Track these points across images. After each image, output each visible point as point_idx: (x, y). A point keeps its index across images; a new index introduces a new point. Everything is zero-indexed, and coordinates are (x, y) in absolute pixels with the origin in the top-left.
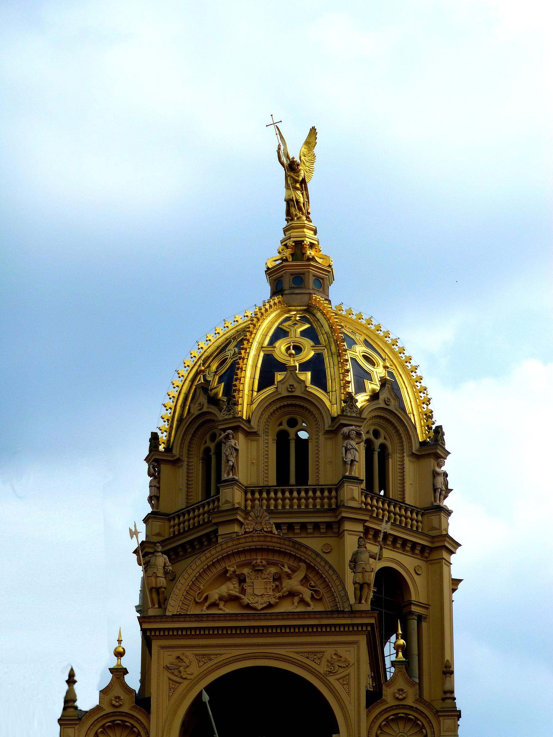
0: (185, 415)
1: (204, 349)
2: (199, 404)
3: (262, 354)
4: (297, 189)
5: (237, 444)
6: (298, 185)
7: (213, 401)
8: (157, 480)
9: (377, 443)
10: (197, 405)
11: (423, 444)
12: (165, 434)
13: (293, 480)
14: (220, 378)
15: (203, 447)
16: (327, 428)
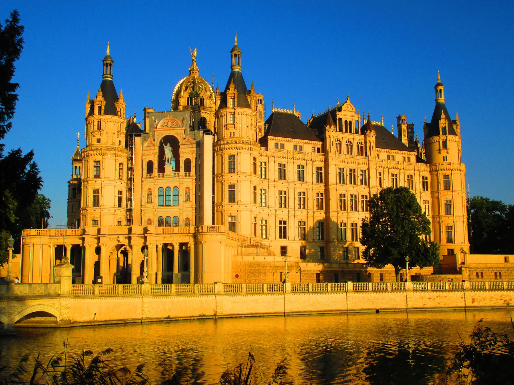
9: (202, 98)
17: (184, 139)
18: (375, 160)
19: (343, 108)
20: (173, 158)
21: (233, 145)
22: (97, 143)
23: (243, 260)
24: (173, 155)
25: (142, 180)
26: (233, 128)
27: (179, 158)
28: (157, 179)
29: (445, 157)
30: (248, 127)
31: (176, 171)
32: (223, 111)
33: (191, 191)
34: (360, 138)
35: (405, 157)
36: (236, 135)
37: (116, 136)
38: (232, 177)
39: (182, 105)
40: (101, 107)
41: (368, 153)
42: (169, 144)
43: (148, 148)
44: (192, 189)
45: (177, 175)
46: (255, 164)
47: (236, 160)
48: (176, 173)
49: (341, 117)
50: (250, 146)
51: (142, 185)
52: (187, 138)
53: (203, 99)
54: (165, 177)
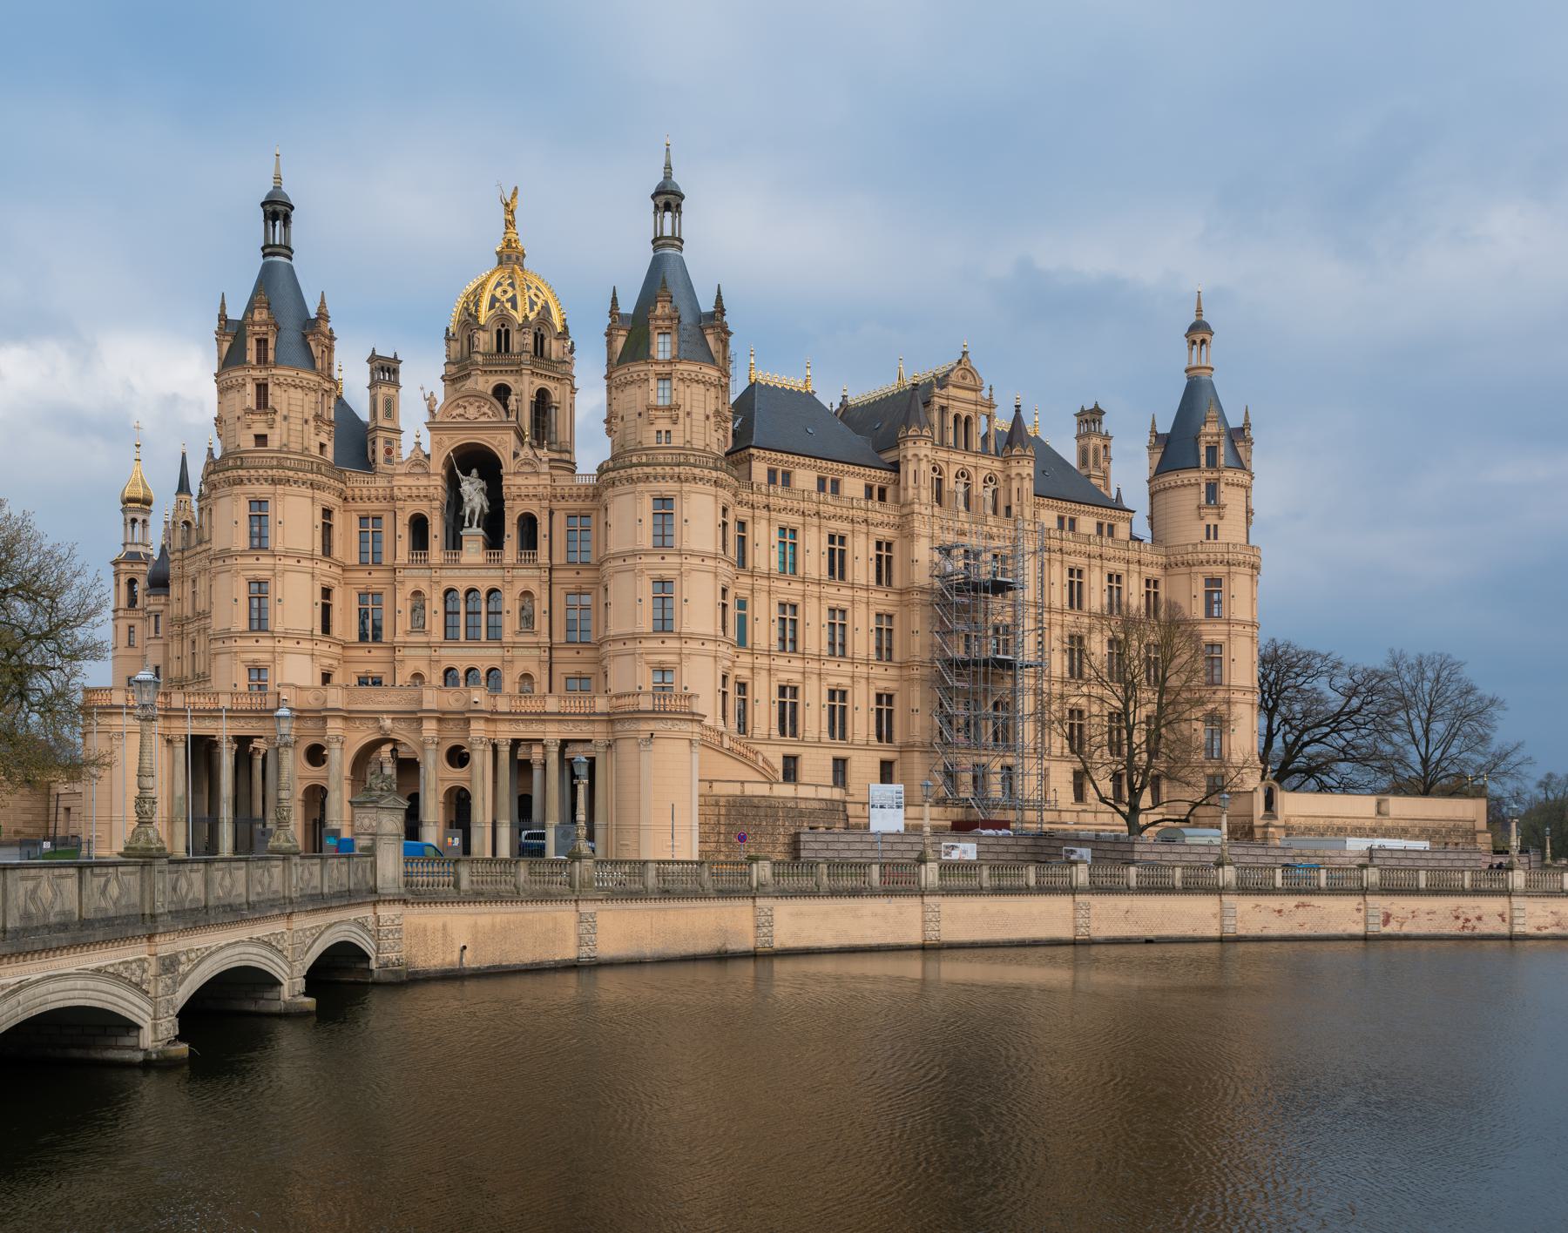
7: (470, 315)
18: (1031, 527)
19: (953, 377)
22: (257, 446)
23: (714, 793)
26: (667, 421)
29: (1212, 528)
30: (707, 417)
32: (638, 369)
34: (993, 465)
35: (1100, 525)
36: (677, 441)
37: (312, 430)
38: (663, 558)
39: (481, 350)
40: (266, 341)
41: (1014, 509)
46: (725, 524)
47: (676, 510)
49: (944, 402)
50: (714, 474)
53: (542, 335)
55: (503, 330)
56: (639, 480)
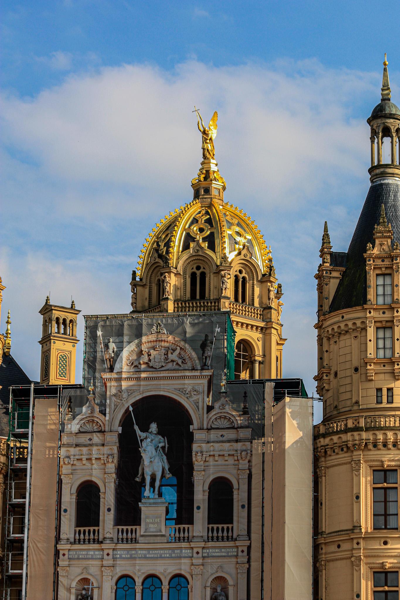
0: (149, 262)
1: (159, 227)
2: (154, 257)
3: (184, 233)
4: (208, 143)
5: (170, 280)
6: (208, 141)
7: (160, 256)
8: (135, 295)
9: (241, 276)
10: (153, 258)
11: (264, 275)
12: (140, 271)
13: (198, 297)
14: (165, 244)
15: (157, 279)
16: (214, 272)
17: (210, 409)
20: (168, 475)
21: (390, 435)
24: (169, 462)
25: (59, 547)
27: (192, 475)
28: (112, 546)
31: (179, 521)
33: (231, 591)
38: (385, 543)
42: (154, 427)
43: (83, 439)
44: (236, 585)
45: (182, 535)
48: (182, 526)
51: (56, 564)
52: (217, 405)
54: (141, 540)
55: (198, 273)
56: (356, 447)
